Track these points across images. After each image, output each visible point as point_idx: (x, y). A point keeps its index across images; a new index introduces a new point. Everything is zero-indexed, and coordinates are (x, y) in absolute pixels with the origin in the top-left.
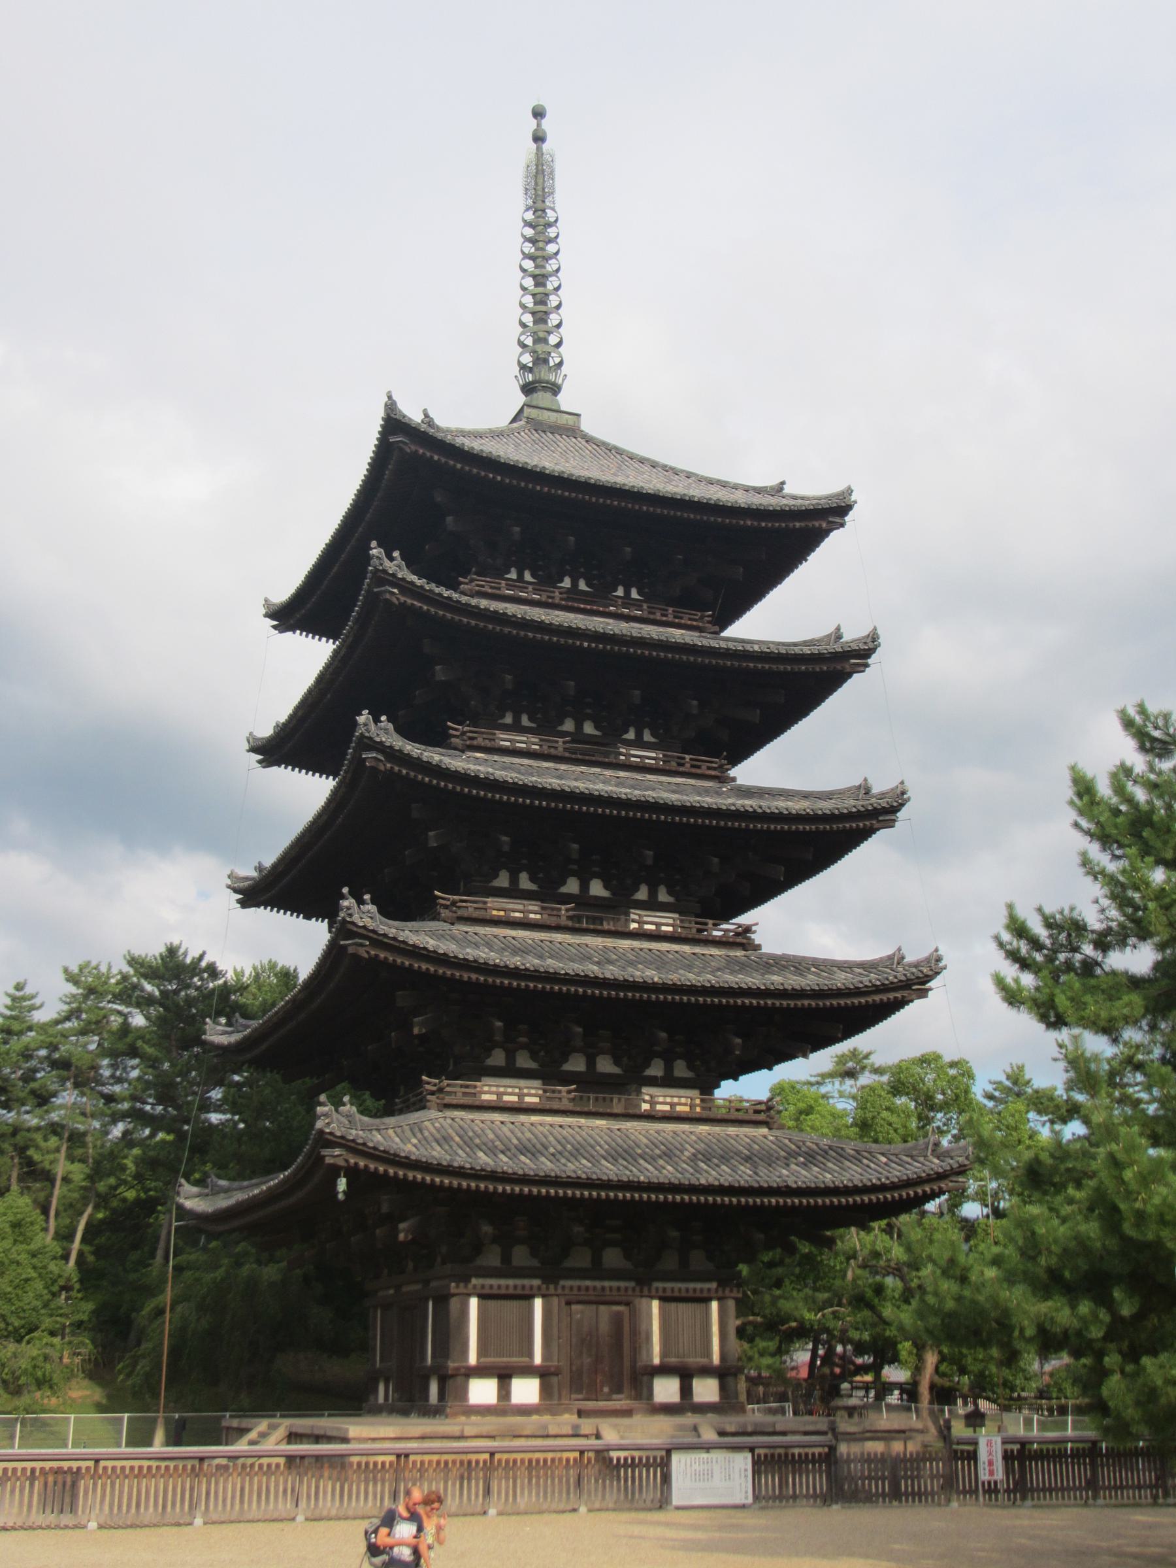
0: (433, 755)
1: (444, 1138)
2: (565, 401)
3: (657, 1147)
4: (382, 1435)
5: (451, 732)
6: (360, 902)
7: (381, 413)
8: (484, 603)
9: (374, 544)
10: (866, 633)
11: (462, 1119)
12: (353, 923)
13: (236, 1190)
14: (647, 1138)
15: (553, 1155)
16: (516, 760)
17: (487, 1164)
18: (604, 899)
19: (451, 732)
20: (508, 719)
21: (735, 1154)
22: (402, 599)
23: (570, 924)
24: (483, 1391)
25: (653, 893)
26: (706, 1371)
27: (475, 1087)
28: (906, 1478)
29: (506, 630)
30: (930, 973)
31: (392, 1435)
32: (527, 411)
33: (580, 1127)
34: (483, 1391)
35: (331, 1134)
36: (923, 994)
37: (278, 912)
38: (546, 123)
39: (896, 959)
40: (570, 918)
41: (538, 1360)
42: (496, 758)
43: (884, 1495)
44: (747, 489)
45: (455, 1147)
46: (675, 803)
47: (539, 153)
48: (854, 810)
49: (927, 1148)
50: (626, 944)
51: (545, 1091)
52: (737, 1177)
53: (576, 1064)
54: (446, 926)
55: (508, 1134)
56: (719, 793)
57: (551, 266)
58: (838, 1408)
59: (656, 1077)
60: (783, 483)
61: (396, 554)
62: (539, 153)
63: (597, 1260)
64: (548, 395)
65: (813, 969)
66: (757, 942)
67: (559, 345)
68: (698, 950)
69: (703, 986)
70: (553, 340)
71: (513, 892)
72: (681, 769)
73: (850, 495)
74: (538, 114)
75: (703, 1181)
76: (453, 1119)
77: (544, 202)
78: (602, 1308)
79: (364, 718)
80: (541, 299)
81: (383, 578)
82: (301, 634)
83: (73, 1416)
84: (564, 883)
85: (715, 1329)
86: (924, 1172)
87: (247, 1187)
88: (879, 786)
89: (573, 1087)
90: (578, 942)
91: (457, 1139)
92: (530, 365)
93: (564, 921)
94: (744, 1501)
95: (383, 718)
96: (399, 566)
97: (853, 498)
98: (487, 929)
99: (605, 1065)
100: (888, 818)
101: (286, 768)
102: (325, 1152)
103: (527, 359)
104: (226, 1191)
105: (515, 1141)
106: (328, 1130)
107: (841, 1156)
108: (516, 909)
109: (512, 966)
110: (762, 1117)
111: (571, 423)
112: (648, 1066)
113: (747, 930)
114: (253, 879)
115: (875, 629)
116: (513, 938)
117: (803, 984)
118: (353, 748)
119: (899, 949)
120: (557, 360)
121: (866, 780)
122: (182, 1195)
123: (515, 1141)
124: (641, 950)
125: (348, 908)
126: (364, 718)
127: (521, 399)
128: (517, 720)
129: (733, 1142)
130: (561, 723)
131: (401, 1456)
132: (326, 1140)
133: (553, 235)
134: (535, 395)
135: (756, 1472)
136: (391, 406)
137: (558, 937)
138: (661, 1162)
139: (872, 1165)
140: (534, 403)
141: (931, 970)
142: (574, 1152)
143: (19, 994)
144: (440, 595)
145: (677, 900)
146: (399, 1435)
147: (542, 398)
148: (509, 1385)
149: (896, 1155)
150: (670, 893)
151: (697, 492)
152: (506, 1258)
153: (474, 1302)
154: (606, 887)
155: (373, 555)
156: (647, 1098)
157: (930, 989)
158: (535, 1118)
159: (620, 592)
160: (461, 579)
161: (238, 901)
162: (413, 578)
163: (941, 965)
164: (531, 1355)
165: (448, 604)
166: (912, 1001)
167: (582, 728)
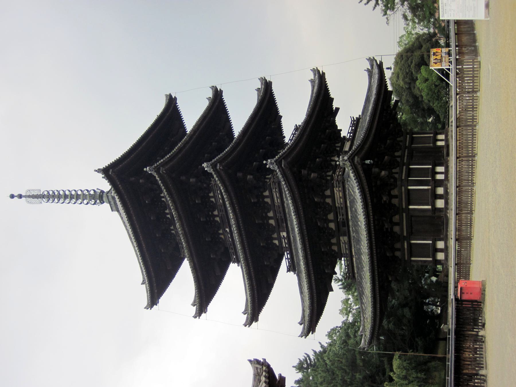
9: (145, 169)
10: (211, 90)
29: (184, 150)
34: (440, 177)
35: (350, 157)
36: (324, 74)
38: (16, 194)
39: (312, 81)
41: (431, 167)
47: (25, 196)
57: (61, 193)
62: (25, 196)
74: (12, 196)
85: (422, 135)
88: (259, 85)
104: (364, 326)
106: (348, 157)
122: (364, 347)
126: (205, 165)
136: (99, 171)
144: (168, 158)
152: (397, 173)
157: (322, 72)
166: (326, 79)
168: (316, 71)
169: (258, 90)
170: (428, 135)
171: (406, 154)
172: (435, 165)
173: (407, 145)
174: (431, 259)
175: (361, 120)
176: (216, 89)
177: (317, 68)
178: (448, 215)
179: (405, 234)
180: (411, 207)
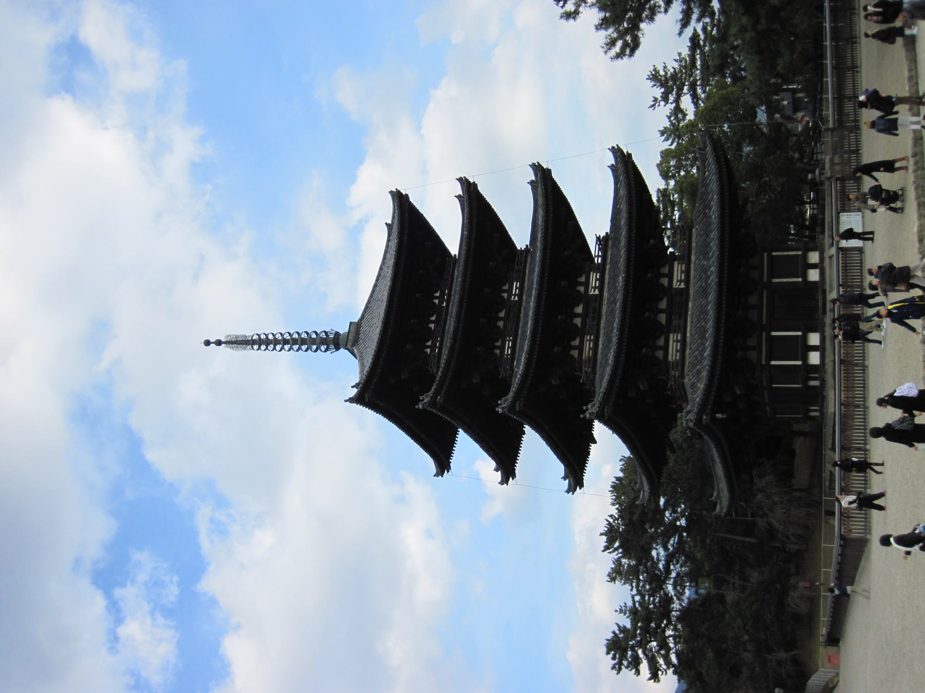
0: (516, 380)
1: (698, 373)
2: (343, 329)
3: (702, 277)
4: (833, 397)
5: (504, 376)
6: (587, 410)
8: (443, 361)
9: (417, 407)
10: (459, 184)
11: (688, 367)
12: (597, 412)
13: (718, 487)
14: (697, 283)
15: (706, 323)
16: (518, 346)
17: (710, 350)
19: (504, 376)
20: (498, 352)
21: (705, 240)
22: (443, 394)
23: (596, 320)
24: (814, 358)
25: (581, 284)
26: (805, 257)
27: (673, 362)
28: (850, 147)
30: (620, 152)
31: (833, 392)
32: (348, 347)
33: (692, 314)
34: (814, 358)
35: (696, 419)
36: (630, 155)
37: (586, 470)
38: (211, 341)
40: (593, 320)
41: (800, 333)
42: (516, 355)
43: (857, 157)
44: (388, 241)
45: (702, 366)
46: (540, 268)
47: (227, 343)
48: (543, 187)
49: (702, 154)
50: (606, 294)
51: (675, 332)
52: (716, 238)
53: (662, 318)
54: (597, 376)
55: (696, 345)
56: (535, 251)
58: (820, 179)
60: (386, 224)
61: (421, 398)
62: (227, 343)
64: (341, 337)
65: (618, 207)
66: (605, 235)
67: (316, 333)
68: (609, 261)
69: (627, 254)
70: (314, 336)
71: (581, 348)
72: (522, 270)
73: (393, 191)
74: (207, 343)
75: (718, 253)
76: (688, 372)
77: (249, 340)
79: (500, 410)
80: (295, 342)
81: (433, 403)
82: (452, 459)
83: (822, 569)
84: (576, 324)
85: (785, 253)
87: (717, 482)
89: (673, 317)
90: (605, 316)
91: (698, 367)
92: (325, 346)
93: (595, 323)
94: (861, 216)
95: (499, 402)
96: (427, 397)
97: (395, 190)
98: (598, 358)
99: (663, 304)
101: (516, 466)
102: (704, 422)
103: (323, 348)
104: (719, 492)
105: (699, 341)
107: (705, 193)
108: (588, 346)
109: (617, 341)
110: (687, 232)
111: (354, 326)
113: (598, 239)
114: (569, 481)
115: (457, 179)
116: (603, 345)
117: (625, 209)
118: (514, 415)
119: (609, 166)
120: (324, 334)
121: (528, 183)
123: (699, 341)
124: (608, 287)
125: (590, 414)
127: (342, 350)
128: (497, 348)
129: (699, 244)
130: (499, 327)
131: (842, 362)
132: (698, 421)
133: (265, 337)
134: (341, 343)
135: (849, 211)
136: (351, 400)
137: (602, 325)
138: (709, 273)
139: (710, 178)
140: (345, 344)
141: (619, 151)
142: (704, 314)
143: (619, 611)
144: (441, 376)
145: (584, 272)
146: (833, 389)
147: (341, 341)
149: (705, 168)
150: (581, 277)
151: (391, 262)
152: (753, 348)
153: (773, 363)
155: (422, 407)
156: (678, 283)
158: (688, 335)
159: (437, 301)
160: (431, 373)
161: (580, 489)
162: (433, 388)
163: (616, 147)
165: (445, 373)
167: (502, 317)
168: (617, 152)
169: (532, 183)
170: (794, 253)
171: (765, 302)
173: (765, 280)
174: (802, 416)
175: (694, 230)
176: (467, 180)
177: (617, 145)
178: (825, 394)
179: (767, 401)
180: (774, 386)
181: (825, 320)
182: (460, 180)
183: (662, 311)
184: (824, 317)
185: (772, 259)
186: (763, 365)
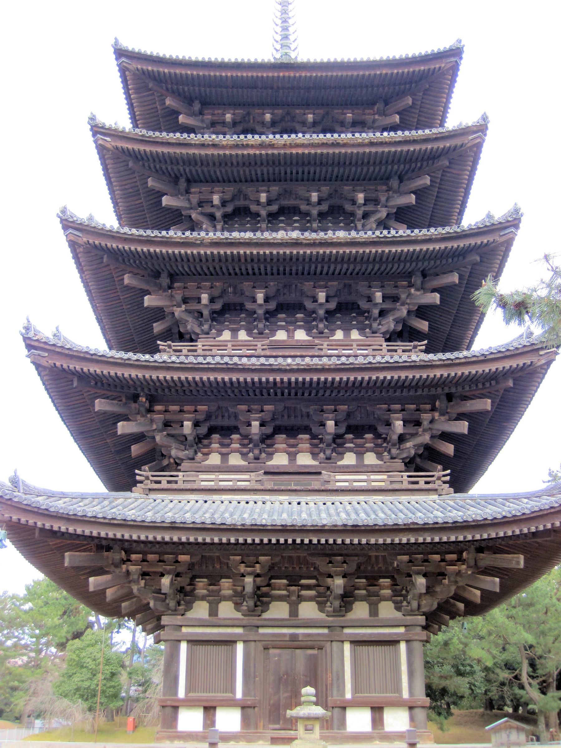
7: (113, 50)
18: (304, 341)
22: (113, 144)
26: (397, 704)
27: (177, 476)
41: (239, 694)
59: (348, 466)
63: (294, 613)
78: (298, 651)
86: (557, 502)
100: (506, 232)
112: (343, 458)
115: (485, 113)
148: (214, 715)
149: (540, 497)
152: (213, 612)
153: (184, 646)
154: (307, 334)
164: (233, 691)
169: (489, 216)
172: (244, 708)
175: (435, 497)
181: (261, 742)
182: (485, 118)
183: (292, 457)
184: (267, 741)
185: (393, 642)
186: (181, 631)
